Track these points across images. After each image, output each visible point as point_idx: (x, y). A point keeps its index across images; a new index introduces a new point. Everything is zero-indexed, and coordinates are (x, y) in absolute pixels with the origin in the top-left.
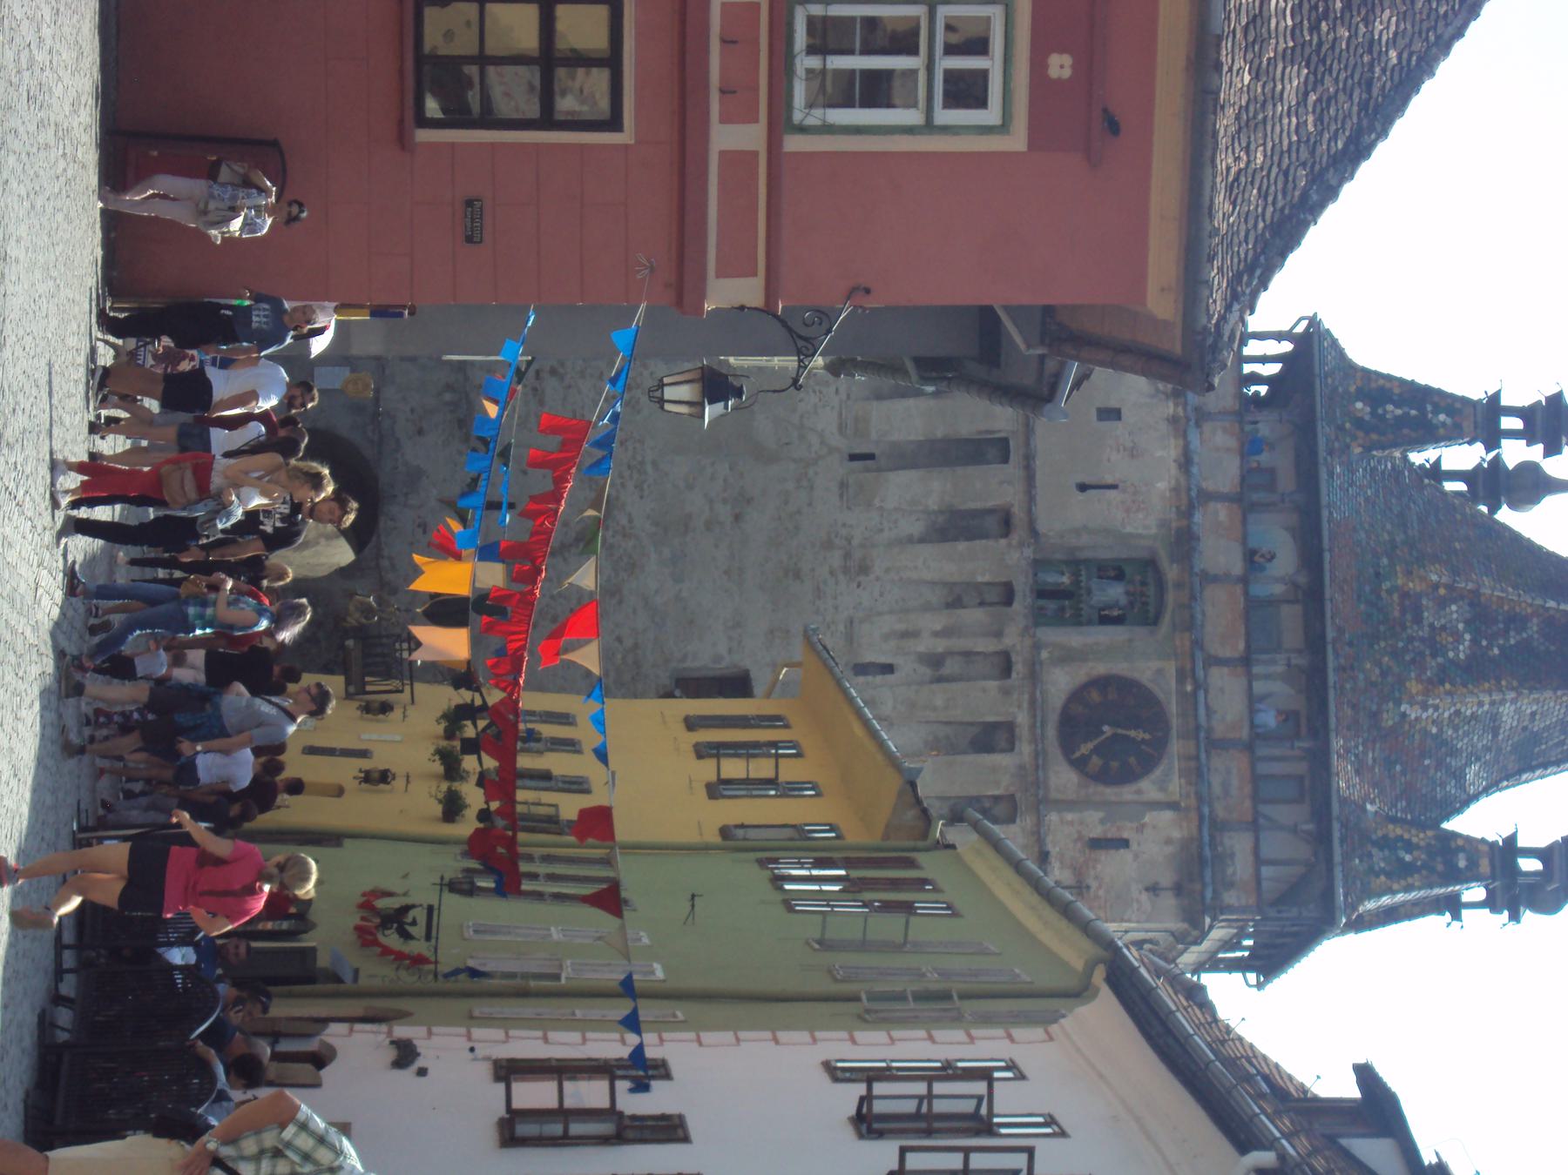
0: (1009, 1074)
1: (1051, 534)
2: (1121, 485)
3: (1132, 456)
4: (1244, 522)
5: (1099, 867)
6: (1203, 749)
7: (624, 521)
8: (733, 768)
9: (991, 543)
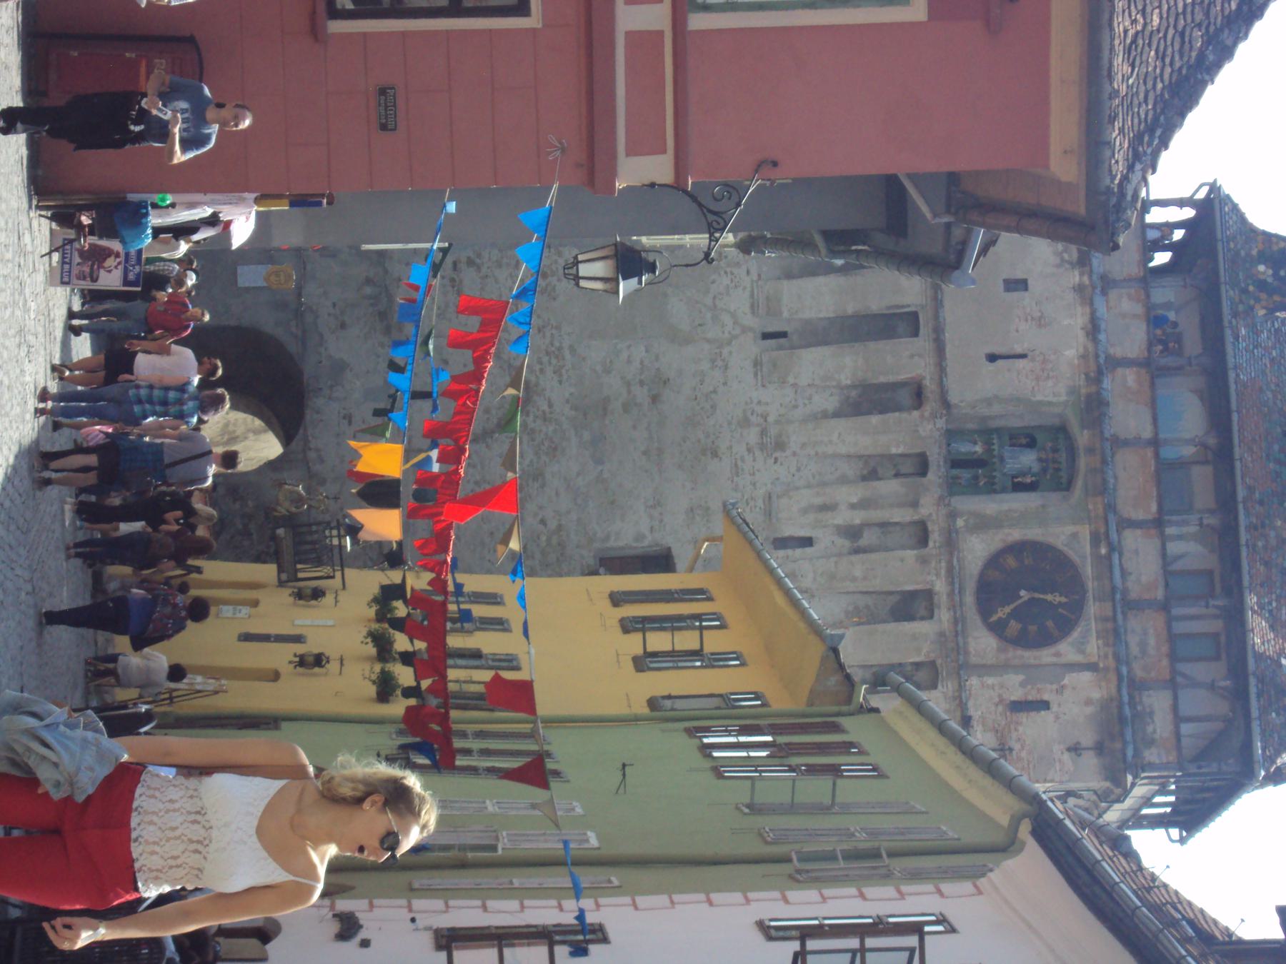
0: (940, 928)
1: (962, 404)
2: (1030, 354)
3: (1040, 326)
4: (1152, 385)
5: (1021, 729)
6: (1119, 610)
7: (545, 408)
8: (659, 641)
9: (905, 415)
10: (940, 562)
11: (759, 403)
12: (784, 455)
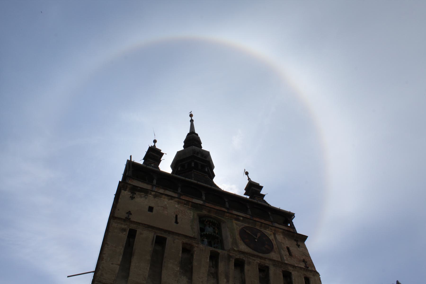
1: (194, 235)
5: (296, 256)
10: (250, 258)
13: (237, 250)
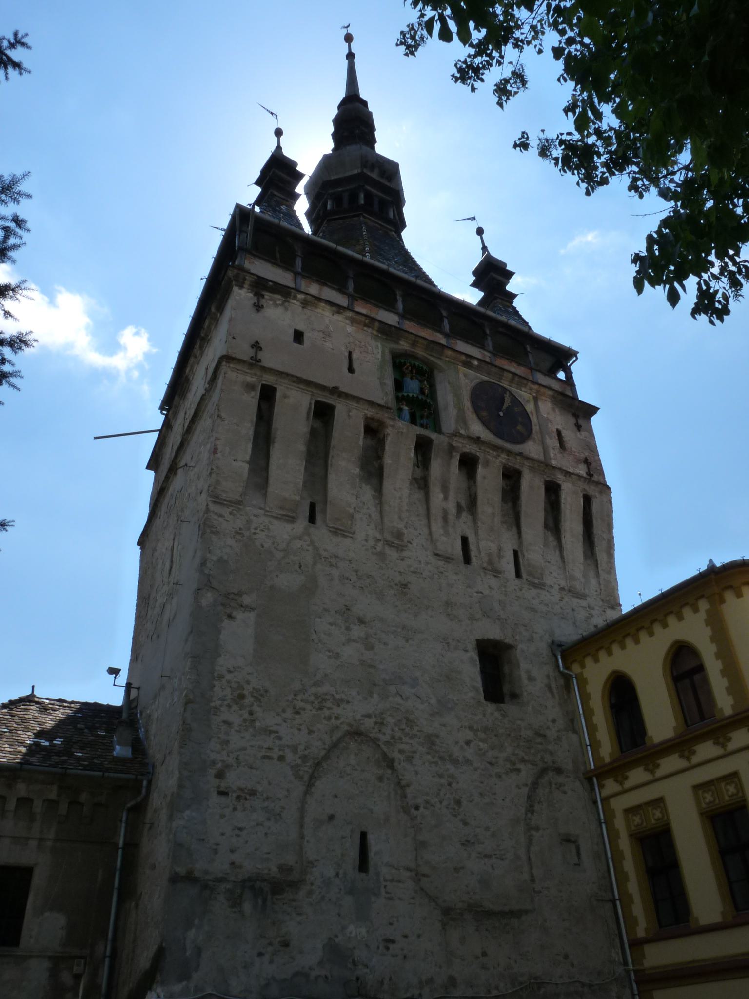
1: (385, 400)
5: (573, 449)
7: (372, 720)
11: (366, 541)
12: (406, 535)
13: (465, 434)
